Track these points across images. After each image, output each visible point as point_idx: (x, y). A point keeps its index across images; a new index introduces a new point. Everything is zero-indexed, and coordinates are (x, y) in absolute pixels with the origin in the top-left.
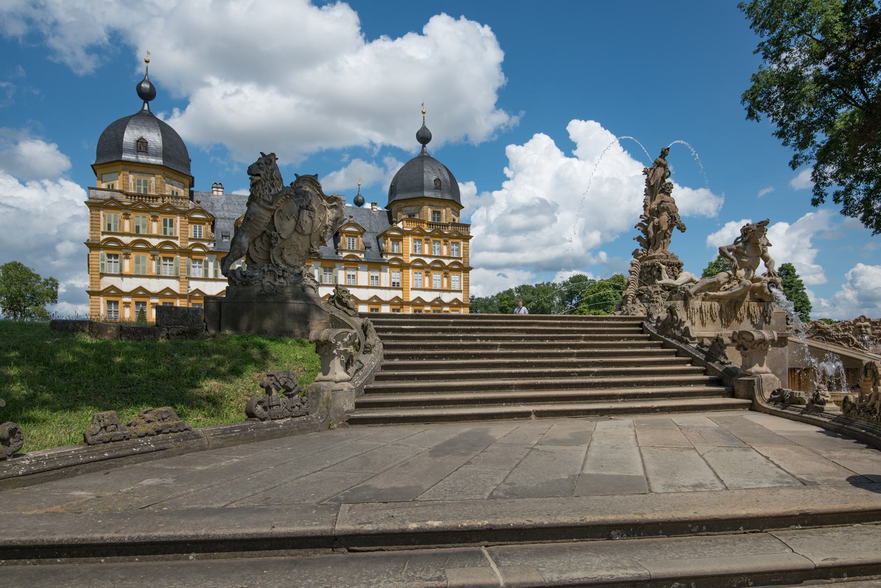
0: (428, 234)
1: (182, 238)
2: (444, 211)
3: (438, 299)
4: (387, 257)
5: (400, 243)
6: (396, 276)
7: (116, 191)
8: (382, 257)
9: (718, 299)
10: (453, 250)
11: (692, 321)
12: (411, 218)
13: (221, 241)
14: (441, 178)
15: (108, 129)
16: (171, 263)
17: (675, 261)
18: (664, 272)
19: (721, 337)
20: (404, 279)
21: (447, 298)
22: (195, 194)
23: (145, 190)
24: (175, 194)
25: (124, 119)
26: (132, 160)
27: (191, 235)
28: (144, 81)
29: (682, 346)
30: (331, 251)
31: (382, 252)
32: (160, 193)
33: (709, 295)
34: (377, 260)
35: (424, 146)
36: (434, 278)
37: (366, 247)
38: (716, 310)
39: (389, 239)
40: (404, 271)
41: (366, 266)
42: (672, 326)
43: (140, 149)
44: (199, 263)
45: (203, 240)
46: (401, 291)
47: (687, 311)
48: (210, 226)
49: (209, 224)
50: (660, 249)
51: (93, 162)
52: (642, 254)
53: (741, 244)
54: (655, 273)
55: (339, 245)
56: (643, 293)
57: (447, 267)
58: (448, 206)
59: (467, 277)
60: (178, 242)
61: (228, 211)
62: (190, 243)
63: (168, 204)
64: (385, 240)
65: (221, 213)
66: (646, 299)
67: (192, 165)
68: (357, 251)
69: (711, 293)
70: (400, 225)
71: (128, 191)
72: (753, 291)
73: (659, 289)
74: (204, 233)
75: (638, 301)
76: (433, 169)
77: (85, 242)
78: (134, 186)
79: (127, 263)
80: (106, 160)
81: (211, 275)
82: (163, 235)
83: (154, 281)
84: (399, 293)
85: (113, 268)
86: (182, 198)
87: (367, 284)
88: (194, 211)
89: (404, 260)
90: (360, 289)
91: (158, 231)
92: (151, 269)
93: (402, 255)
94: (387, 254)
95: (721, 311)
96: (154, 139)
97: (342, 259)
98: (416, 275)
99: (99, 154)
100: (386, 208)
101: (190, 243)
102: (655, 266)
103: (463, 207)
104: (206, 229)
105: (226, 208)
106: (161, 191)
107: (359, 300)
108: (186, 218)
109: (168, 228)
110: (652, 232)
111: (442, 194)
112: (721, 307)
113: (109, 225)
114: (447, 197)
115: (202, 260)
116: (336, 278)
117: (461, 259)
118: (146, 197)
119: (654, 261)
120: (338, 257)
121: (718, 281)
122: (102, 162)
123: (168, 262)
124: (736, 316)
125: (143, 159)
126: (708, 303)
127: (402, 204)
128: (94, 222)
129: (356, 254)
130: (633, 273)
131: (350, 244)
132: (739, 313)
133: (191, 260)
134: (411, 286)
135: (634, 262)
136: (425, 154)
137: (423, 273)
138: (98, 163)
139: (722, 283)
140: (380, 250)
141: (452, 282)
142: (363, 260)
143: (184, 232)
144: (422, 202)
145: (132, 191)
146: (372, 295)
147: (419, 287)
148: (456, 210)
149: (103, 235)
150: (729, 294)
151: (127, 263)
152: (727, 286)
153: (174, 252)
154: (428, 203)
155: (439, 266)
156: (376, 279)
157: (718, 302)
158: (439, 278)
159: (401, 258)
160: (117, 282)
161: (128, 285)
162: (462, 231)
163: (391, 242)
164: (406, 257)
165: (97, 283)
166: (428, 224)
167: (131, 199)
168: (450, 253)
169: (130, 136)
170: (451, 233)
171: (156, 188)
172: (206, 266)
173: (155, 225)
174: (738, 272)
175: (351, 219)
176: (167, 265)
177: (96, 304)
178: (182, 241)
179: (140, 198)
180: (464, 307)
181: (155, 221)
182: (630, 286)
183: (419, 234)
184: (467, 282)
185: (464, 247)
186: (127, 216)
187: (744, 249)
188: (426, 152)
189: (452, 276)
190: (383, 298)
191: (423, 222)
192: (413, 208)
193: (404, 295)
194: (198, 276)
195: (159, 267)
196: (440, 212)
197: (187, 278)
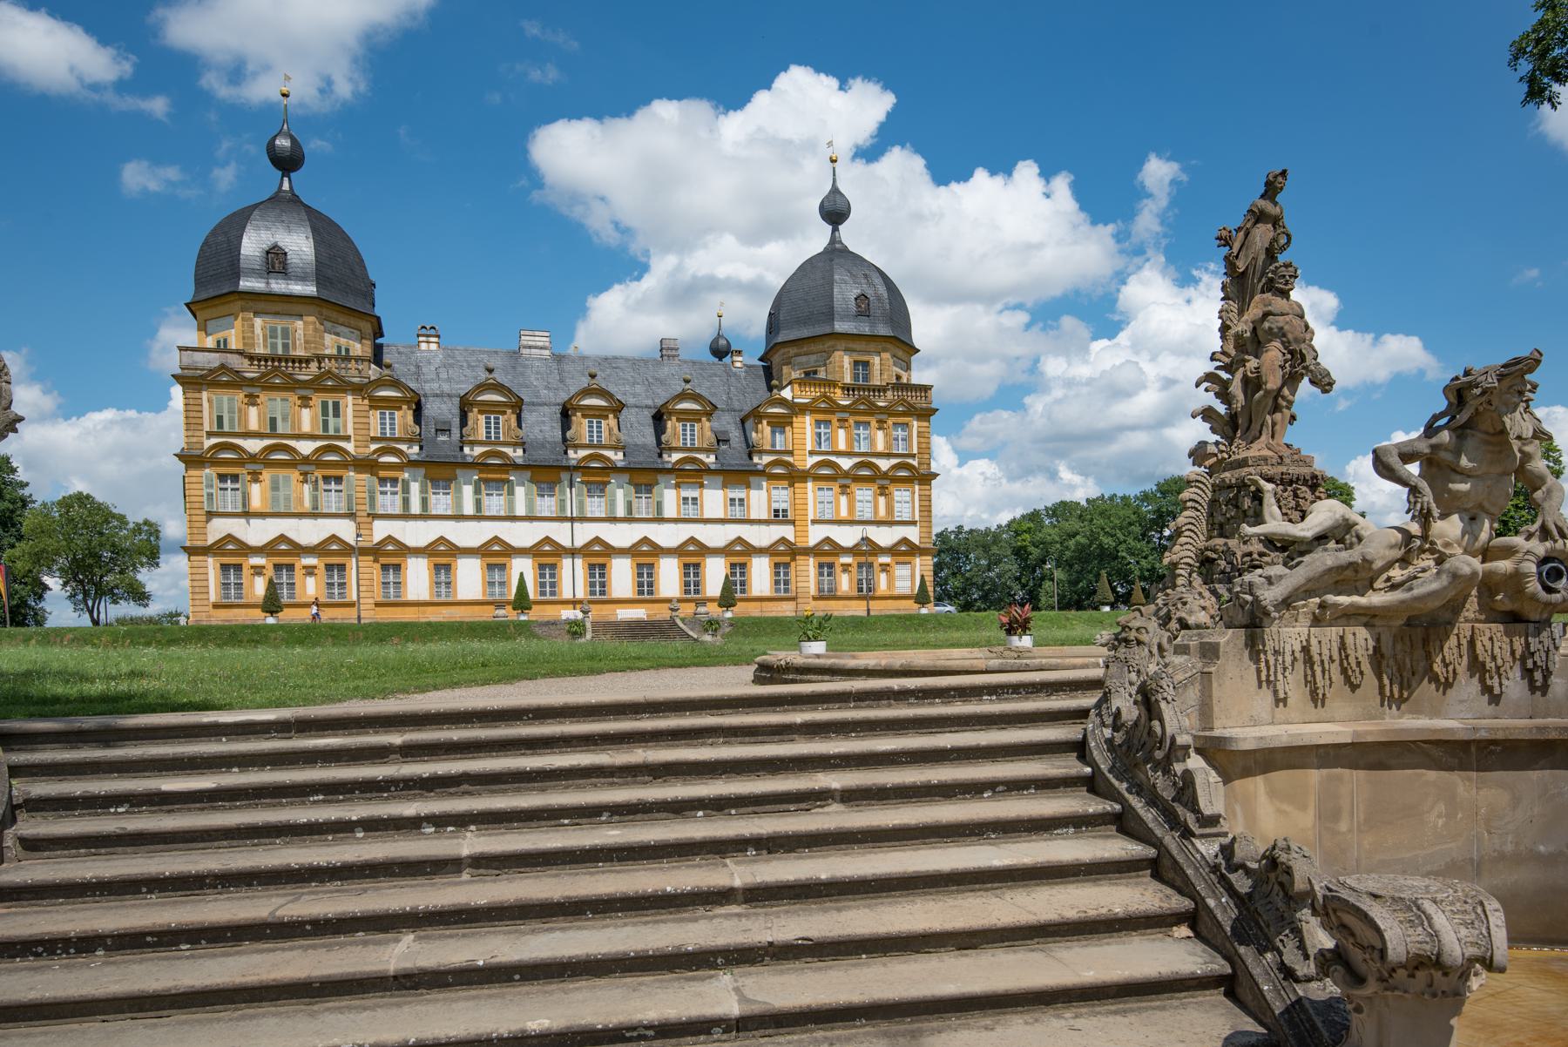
0: (844, 409)
1: (360, 438)
2: (877, 360)
3: (866, 540)
4: (760, 459)
5: (788, 429)
6: (782, 496)
7: (232, 352)
8: (751, 458)
9: (1368, 617)
10: (896, 439)
11: (1276, 692)
12: (809, 378)
14: (869, 292)
15: (214, 233)
16: (339, 488)
17: (1305, 471)
18: (1269, 500)
19: (1283, 857)
20: (797, 501)
21: (885, 537)
22: (385, 350)
23: (285, 346)
24: (343, 353)
25: (243, 210)
26: (257, 289)
27: (375, 431)
28: (280, 133)
29: (1171, 840)
30: (650, 451)
31: (751, 450)
32: (313, 351)
33: (1336, 605)
35: (835, 230)
36: (858, 498)
37: (718, 441)
38: (1361, 652)
39: (765, 422)
40: (796, 485)
41: (720, 479)
42: (1149, 758)
43: (273, 267)
44: (391, 486)
46: (792, 527)
47: (1257, 661)
48: (411, 412)
49: (409, 408)
50: (1263, 438)
51: (188, 301)
52: (1216, 455)
53: (1445, 436)
54: (1247, 503)
55: (664, 438)
56: (1215, 556)
57: (885, 475)
58: (885, 350)
59: (927, 492)
60: (350, 447)
61: (449, 380)
62: (374, 447)
63: (329, 372)
64: (757, 424)
65: (436, 385)
66: (1223, 572)
67: (378, 294)
68: (699, 450)
69: (1344, 600)
70: (787, 393)
71: (252, 351)
72: (1488, 586)
73: (1257, 547)
74: (399, 425)
75: (1197, 581)
76: (853, 276)
77: (178, 451)
78: (265, 340)
79: (255, 489)
80: (212, 293)
81: (416, 508)
83: (307, 523)
84: (787, 532)
86: (358, 359)
87: (722, 516)
88: (380, 383)
89: (796, 463)
90: (709, 526)
91: (312, 427)
92: (301, 500)
93: (791, 453)
94: (761, 452)
95: (1377, 657)
96: (299, 245)
97: (670, 466)
98: (821, 493)
99: (200, 282)
100: (761, 359)
102: (1246, 486)
103: (918, 351)
104: (404, 417)
105: (444, 375)
106: (315, 348)
108: (363, 398)
109: (331, 419)
110: (1241, 397)
111: (873, 325)
112: (1378, 640)
113: (220, 419)
114: (883, 330)
116: (659, 505)
117: (913, 456)
118: (287, 361)
119: (1244, 471)
120: (663, 463)
121: (1364, 560)
122: (204, 296)
123: (333, 486)
124: (1429, 668)
125: (278, 286)
126: (1333, 632)
127: (792, 351)
128: (191, 414)
129: (698, 456)
130: (1189, 504)
131: (685, 435)
132: (1439, 660)
133: (376, 480)
134: (811, 517)
135: (1193, 477)
136: (837, 246)
137: (836, 487)
138: (197, 299)
139: (1378, 564)
140: (748, 446)
141: (896, 505)
142: (713, 467)
143: (362, 426)
144: (831, 343)
146: (733, 537)
147: (828, 517)
148: (903, 357)
149: (208, 438)
150: (1403, 602)
151: (255, 489)
152: (1397, 573)
153: (344, 465)
154: (843, 344)
155: (867, 474)
156: (740, 505)
157: (1366, 625)
158: (870, 498)
159: (790, 459)
160: (236, 527)
161: (257, 533)
162: (911, 397)
163: (769, 428)
164: (800, 458)
165: (201, 531)
166: (843, 388)
167: (259, 366)
168: (891, 445)
169: (252, 244)
170: (893, 404)
171: (306, 342)
172: (406, 490)
173: (306, 413)
174: (1438, 526)
175: (688, 386)
176: (331, 491)
177: (201, 570)
178: (358, 443)
179: (276, 364)
180: (921, 555)
181: (306, 406)
182: (1182, 540)
183: (826, 411)
184: (927, 503)
185: (919, 432)
186: (252, 400)
187: (1457, 453)
188: (841, 242)
189: (896, 493)
191: (832, 384)
192: (813, 358)
193: (799, 534)
194: (389, 512)
195: (317, 497)
196: (868, 362)
197: (369, 515)
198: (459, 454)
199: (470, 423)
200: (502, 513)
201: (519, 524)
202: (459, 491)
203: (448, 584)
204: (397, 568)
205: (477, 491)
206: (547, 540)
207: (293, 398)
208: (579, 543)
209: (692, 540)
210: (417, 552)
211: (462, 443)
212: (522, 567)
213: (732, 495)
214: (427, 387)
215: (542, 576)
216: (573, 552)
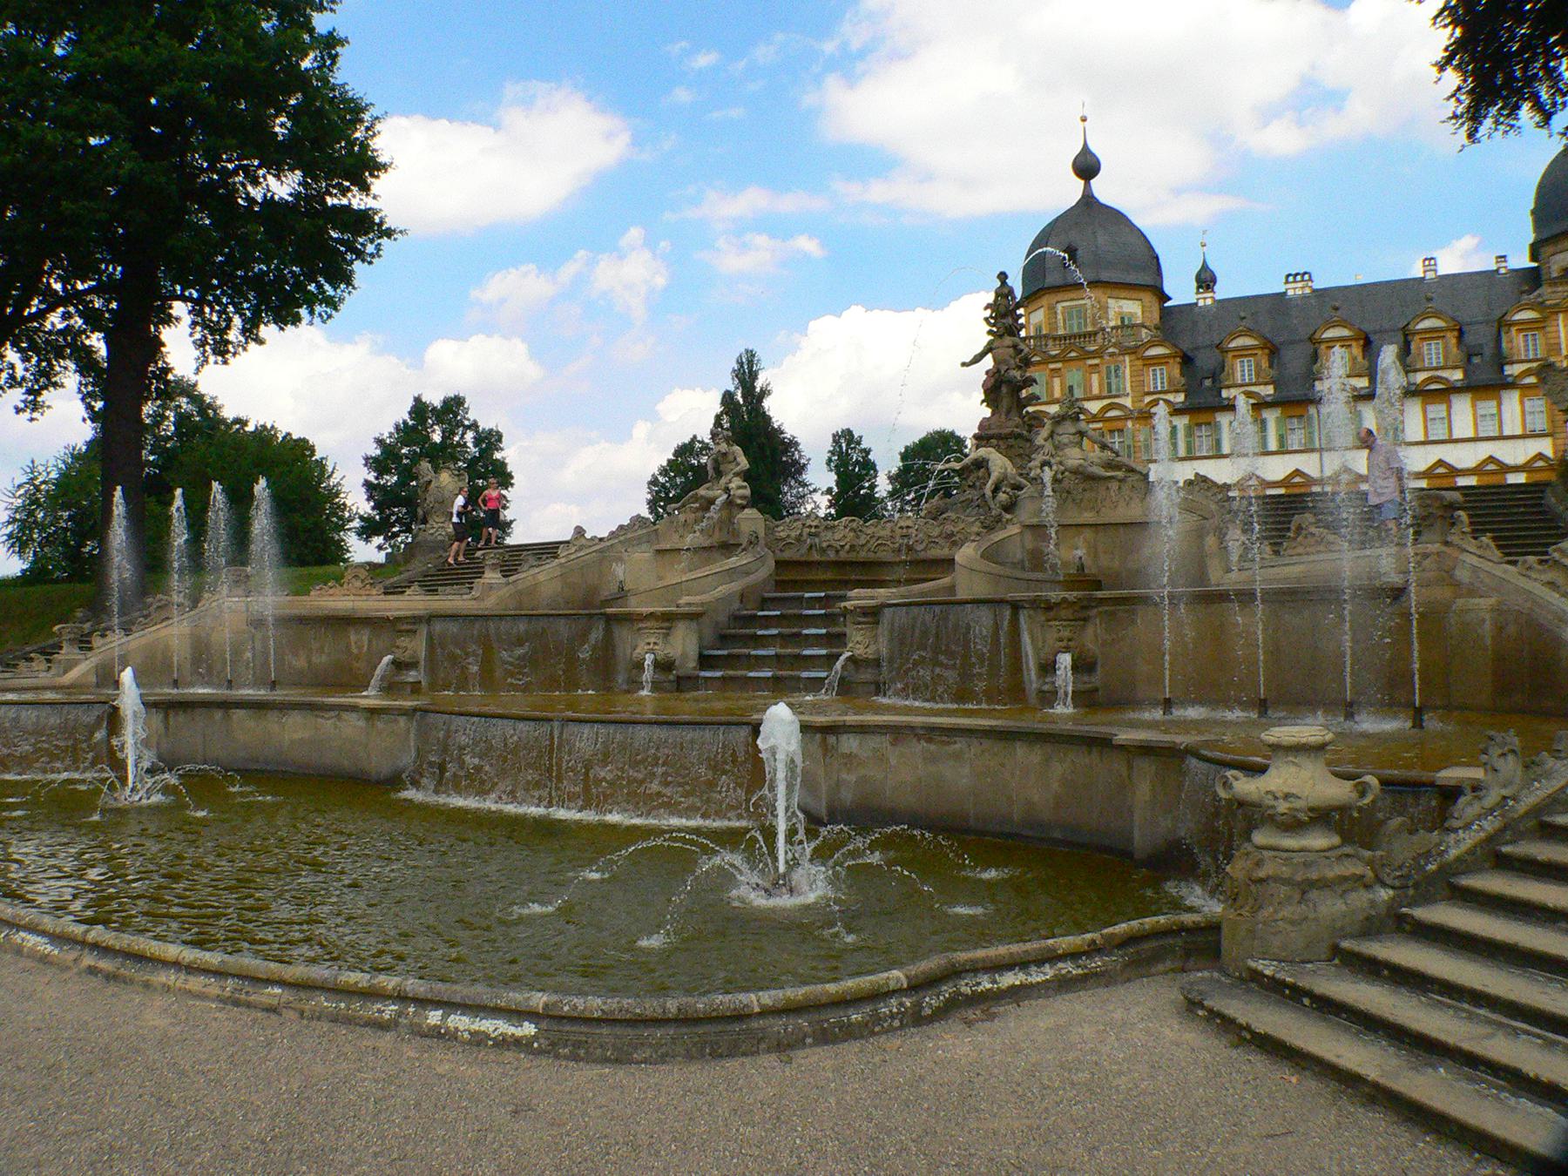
8: (1502, 371)
23: (1079, 327)
34: (1491, 380)
45: (1166, 392)
60: (1127, 402)
62: (1148, 399)
82: (1105, 393)
87: (1471, 434)
90: (1459, 446)
91: (1100, 391)
94: (1512, 363)
101: (1148, 399)
107: (1456, 469)
109: (1113, 380)
145: (1061, 332)
153: (1127, 418)
190: (1509, 460)
199: (1226, 369)
208: (1328, 473)
209: (1441, 463)
213: (1480, 412)
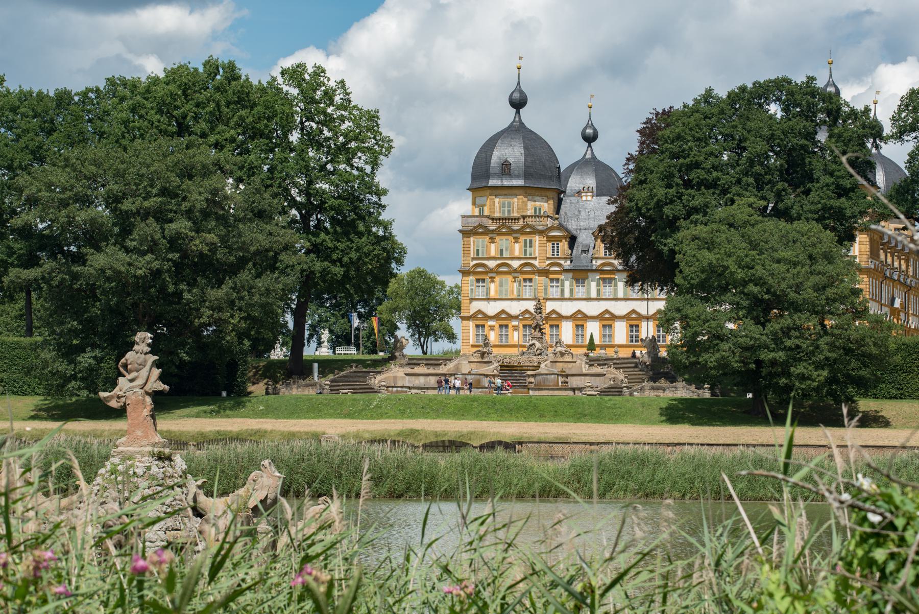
13: (579, 257)
23: (509, 211)
27: (549, 254)
60: (536, 263)
62: (548, 262)
79: (492, 286)
81: (567, 295)
83: (515, 303)
85: (480, 292)
92: (512, 291)
104: (564, 245)
105: (592, 216)
109: (528, 249)
113: (478, 250)
115: (557, 280)
123: (528, 284)
145: (497, 215)
151: (492, 286)
153: (533, 273)
172: (563, 285)
173: (517, 246)
181: (517, 242)
186: (492, 240)
194: (555, 296)
198: (590, 264)
200: (612, 297)
201: (619, 303)
202: (589, 285)
203: (582, 335)
204: (557, 326)
205: (598, 285)
206: (634, 311)
207: (511, 238)
208: (651, 312)
210: (567, 318)
211: (593, 258)
212: (593, 329)
214: (582, 224)
215: (632, 331)
216: (647, 318)
